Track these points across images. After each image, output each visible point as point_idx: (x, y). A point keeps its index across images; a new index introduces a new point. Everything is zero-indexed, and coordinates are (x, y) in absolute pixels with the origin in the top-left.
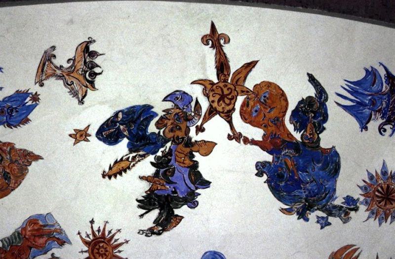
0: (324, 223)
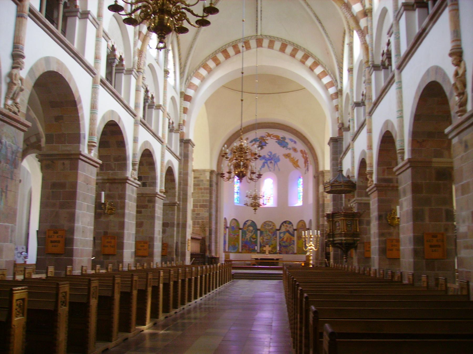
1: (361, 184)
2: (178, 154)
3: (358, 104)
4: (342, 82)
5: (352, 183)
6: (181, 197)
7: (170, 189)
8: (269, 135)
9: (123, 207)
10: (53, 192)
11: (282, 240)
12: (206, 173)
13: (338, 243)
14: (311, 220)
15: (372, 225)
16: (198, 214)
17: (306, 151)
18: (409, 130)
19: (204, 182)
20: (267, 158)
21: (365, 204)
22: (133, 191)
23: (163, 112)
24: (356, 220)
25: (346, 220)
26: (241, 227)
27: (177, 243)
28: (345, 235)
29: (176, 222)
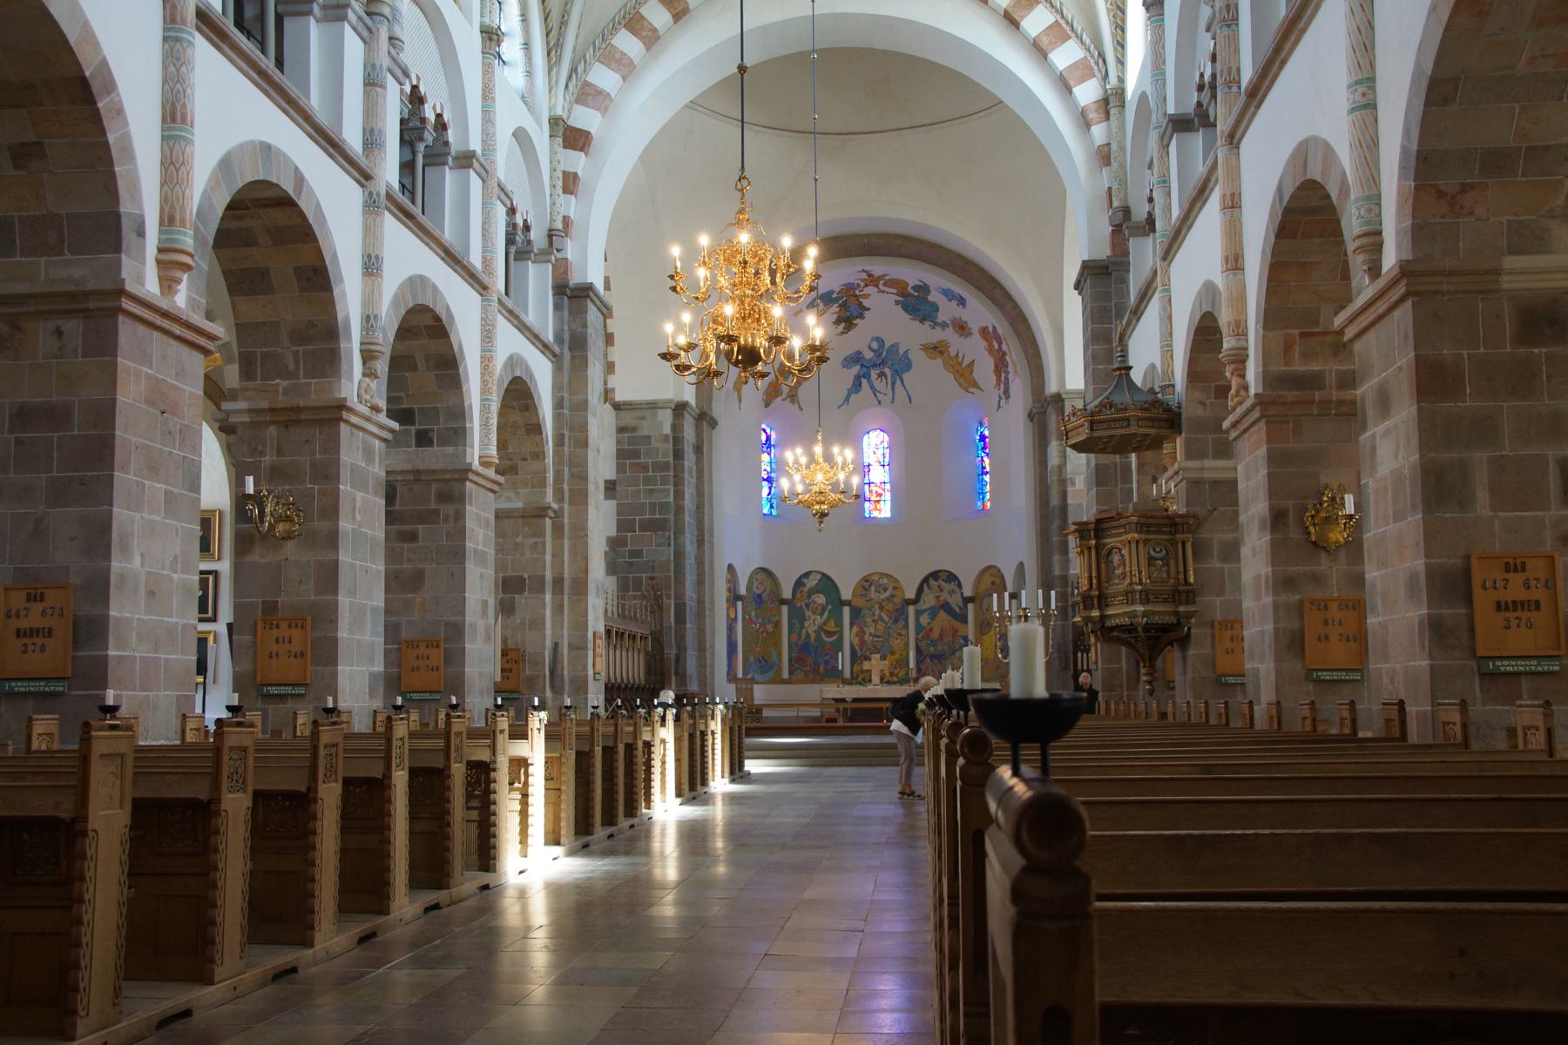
0: (934, 328)
1: (1200, 412)
2: (549, 336)
3: (1180, 124)
4: (1121, 62)
5: (1168, 410)
6: (566, 487)
7: (525, 459)
8: (872, 280)
9: (332, 511)
10: (18, 442)
11: (927, 636)
12: (660, 412)
13: (1117, 627)
14: (1021, 565)
15: (1245, 551)
16: (636, 554)
17: (1000, 331)
18: (1405, 151)
19: (655, 443)
20: (870, 360)
21: (1216, 483)
22: (368, 453)
23: (483, 181)
24: (1184, 543)
25: (1146, 542)
26: (787, 593)
27: (556, 646)
28: (1146, 597)
29: (549, 575)
